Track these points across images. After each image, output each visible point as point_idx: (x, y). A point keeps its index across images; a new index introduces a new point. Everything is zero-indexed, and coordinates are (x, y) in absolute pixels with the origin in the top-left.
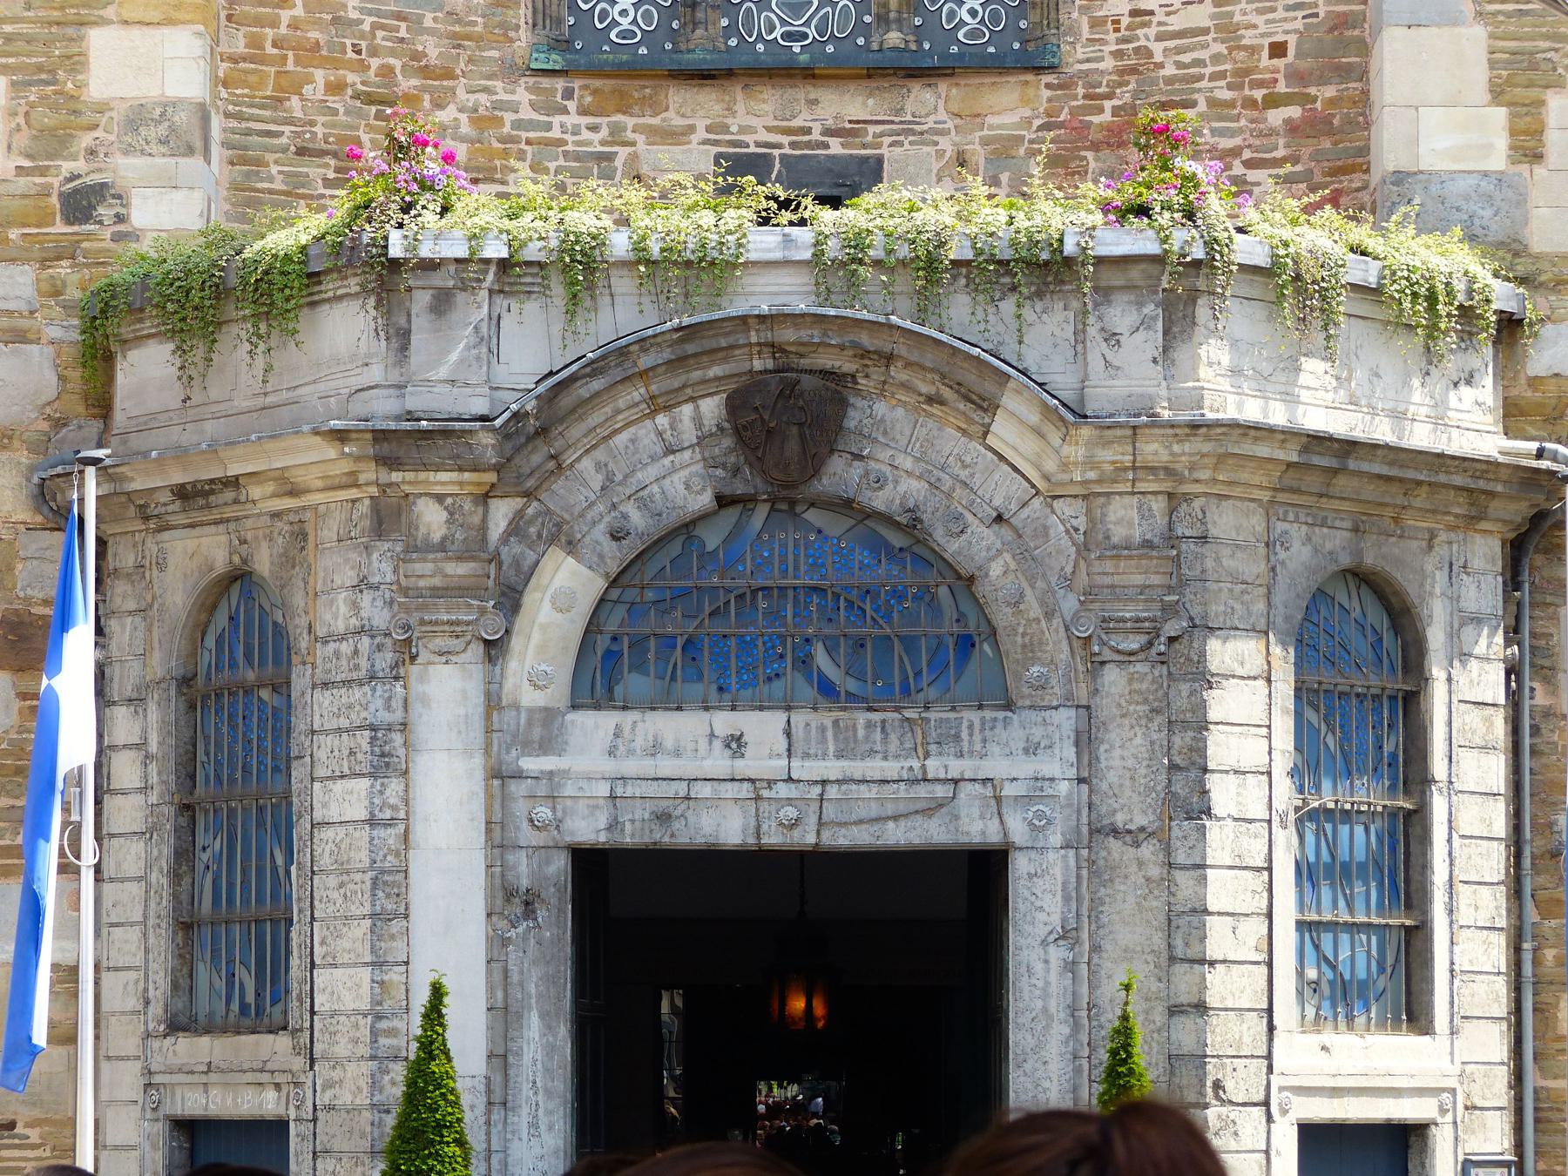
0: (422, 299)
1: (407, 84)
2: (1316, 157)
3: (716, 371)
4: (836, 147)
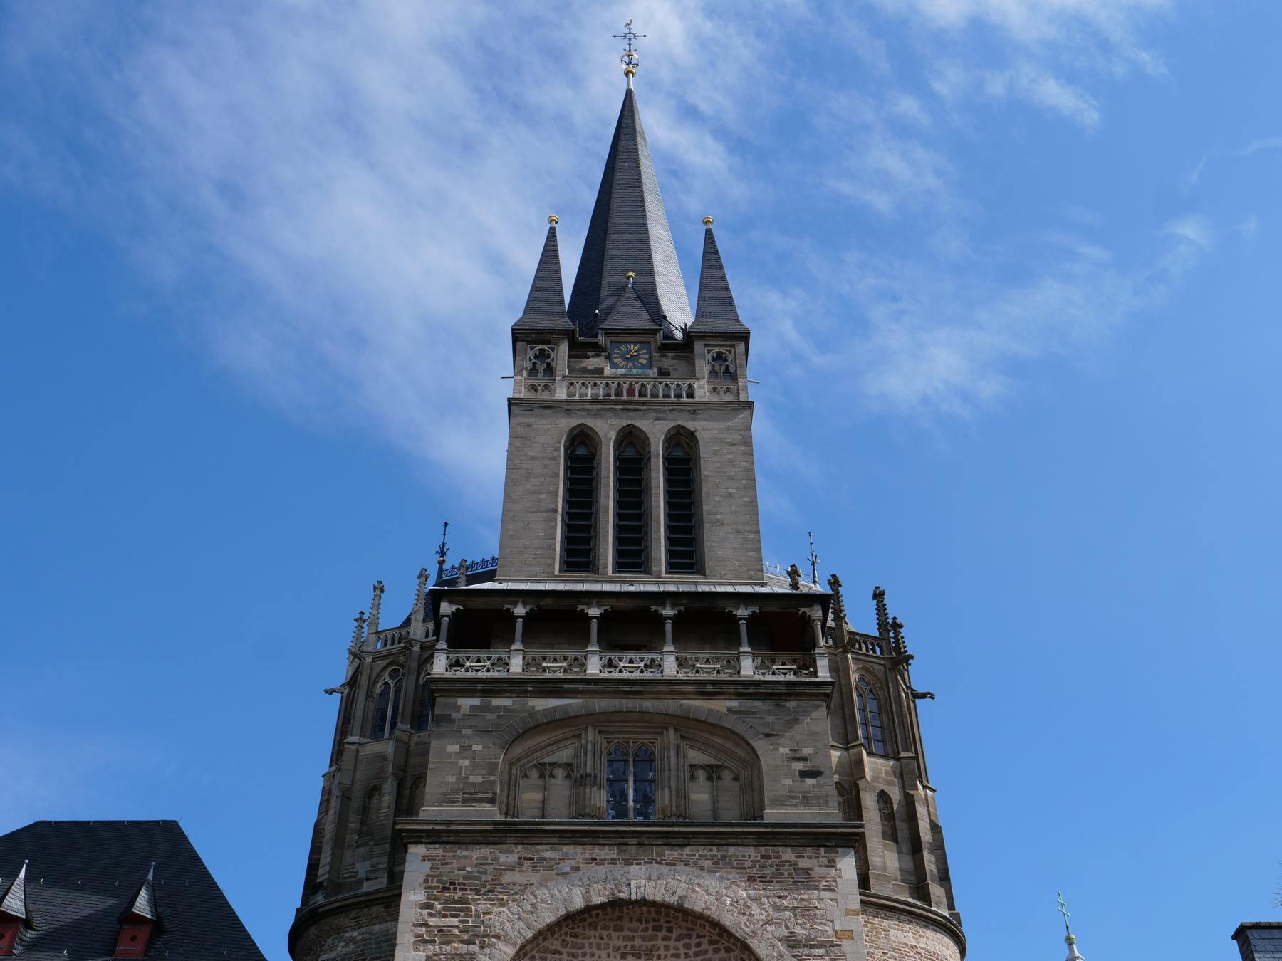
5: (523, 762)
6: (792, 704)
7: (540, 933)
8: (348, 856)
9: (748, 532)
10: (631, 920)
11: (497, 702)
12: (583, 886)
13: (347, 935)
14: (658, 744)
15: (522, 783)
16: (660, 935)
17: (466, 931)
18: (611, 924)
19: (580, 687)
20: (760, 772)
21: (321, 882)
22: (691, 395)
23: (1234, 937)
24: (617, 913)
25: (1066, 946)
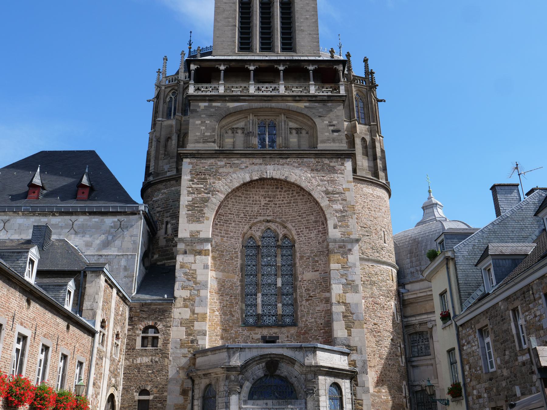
0: (232, 352)
1: (228, 328)
2: (326, 336)
3: (264, 360)
4: (274, 335)
5: (225, 127)
6: (329, 104)
7: (234, 190)
8: (161, 163)
9: (314, 34)
10: (267, 185)
11: (214, 104)
12: (249, 173)
13: (162, 191)
14: (277, 120)
15: (225, 135)
16: (278, 190)
17: (206, 189)
18: (260, 187)
19: (247, 98)
20: (317, 131)
21: (151, 173)
23: (491, 189)
24: (262, 183)
25: (428, 193)
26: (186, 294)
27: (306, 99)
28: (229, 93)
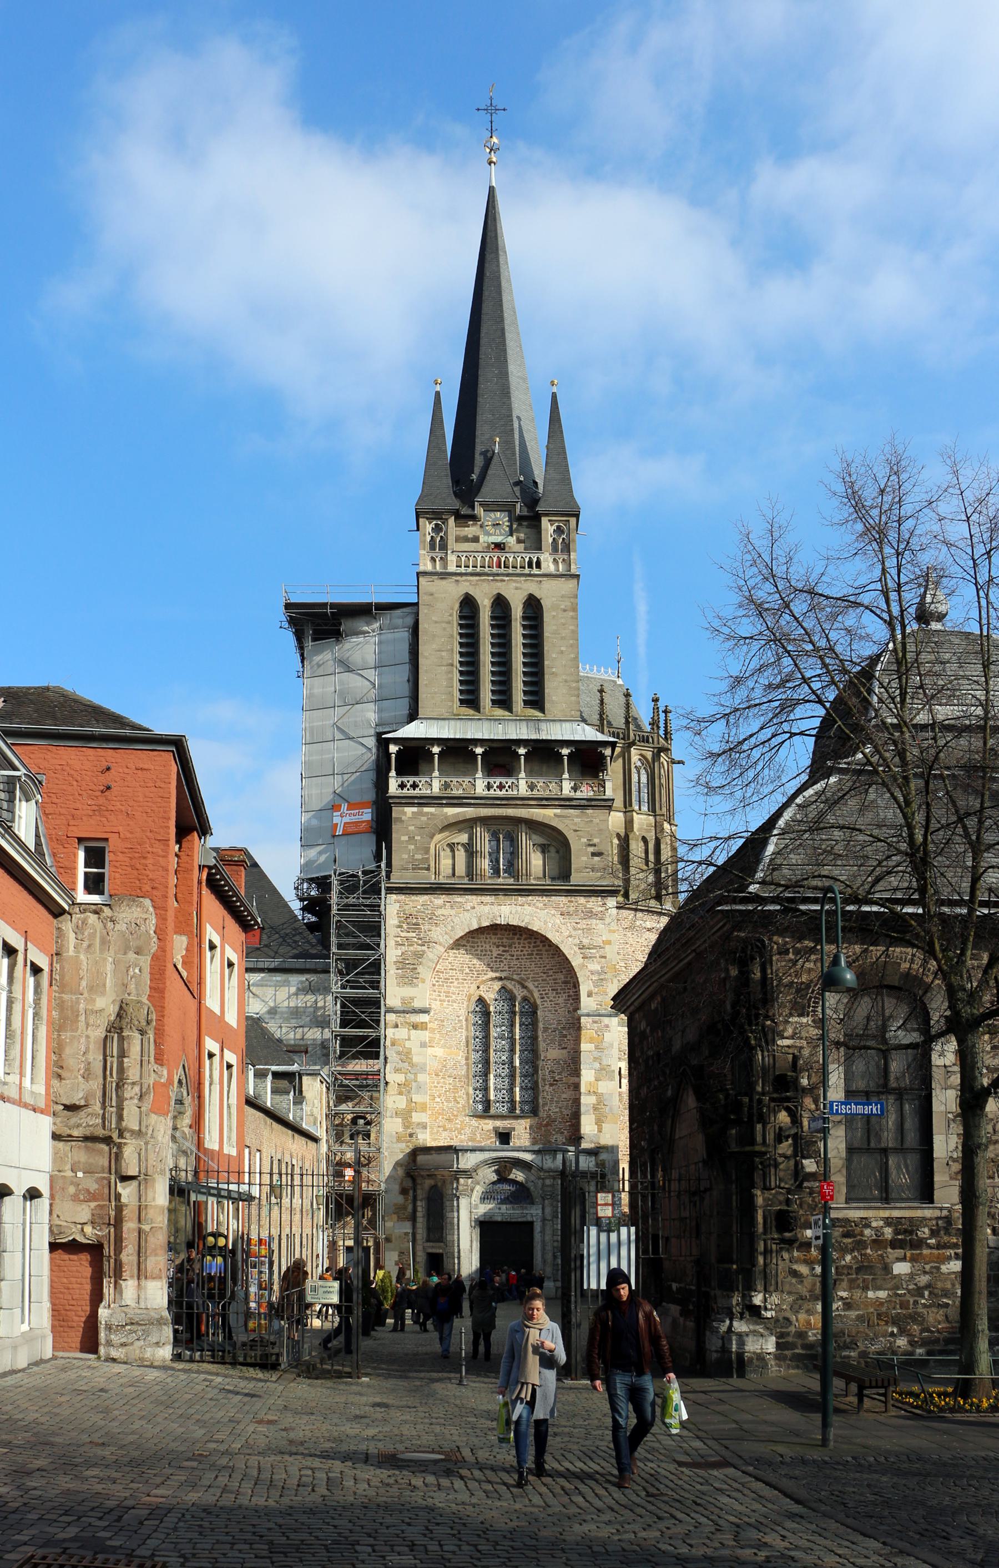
6: (590, 811)
7: (457, 940)
11: (426, 809)
19: (472, 801)
22: (538, 565)
26: (400, 1078)
27: (557, 803)
28: (449, 793)
